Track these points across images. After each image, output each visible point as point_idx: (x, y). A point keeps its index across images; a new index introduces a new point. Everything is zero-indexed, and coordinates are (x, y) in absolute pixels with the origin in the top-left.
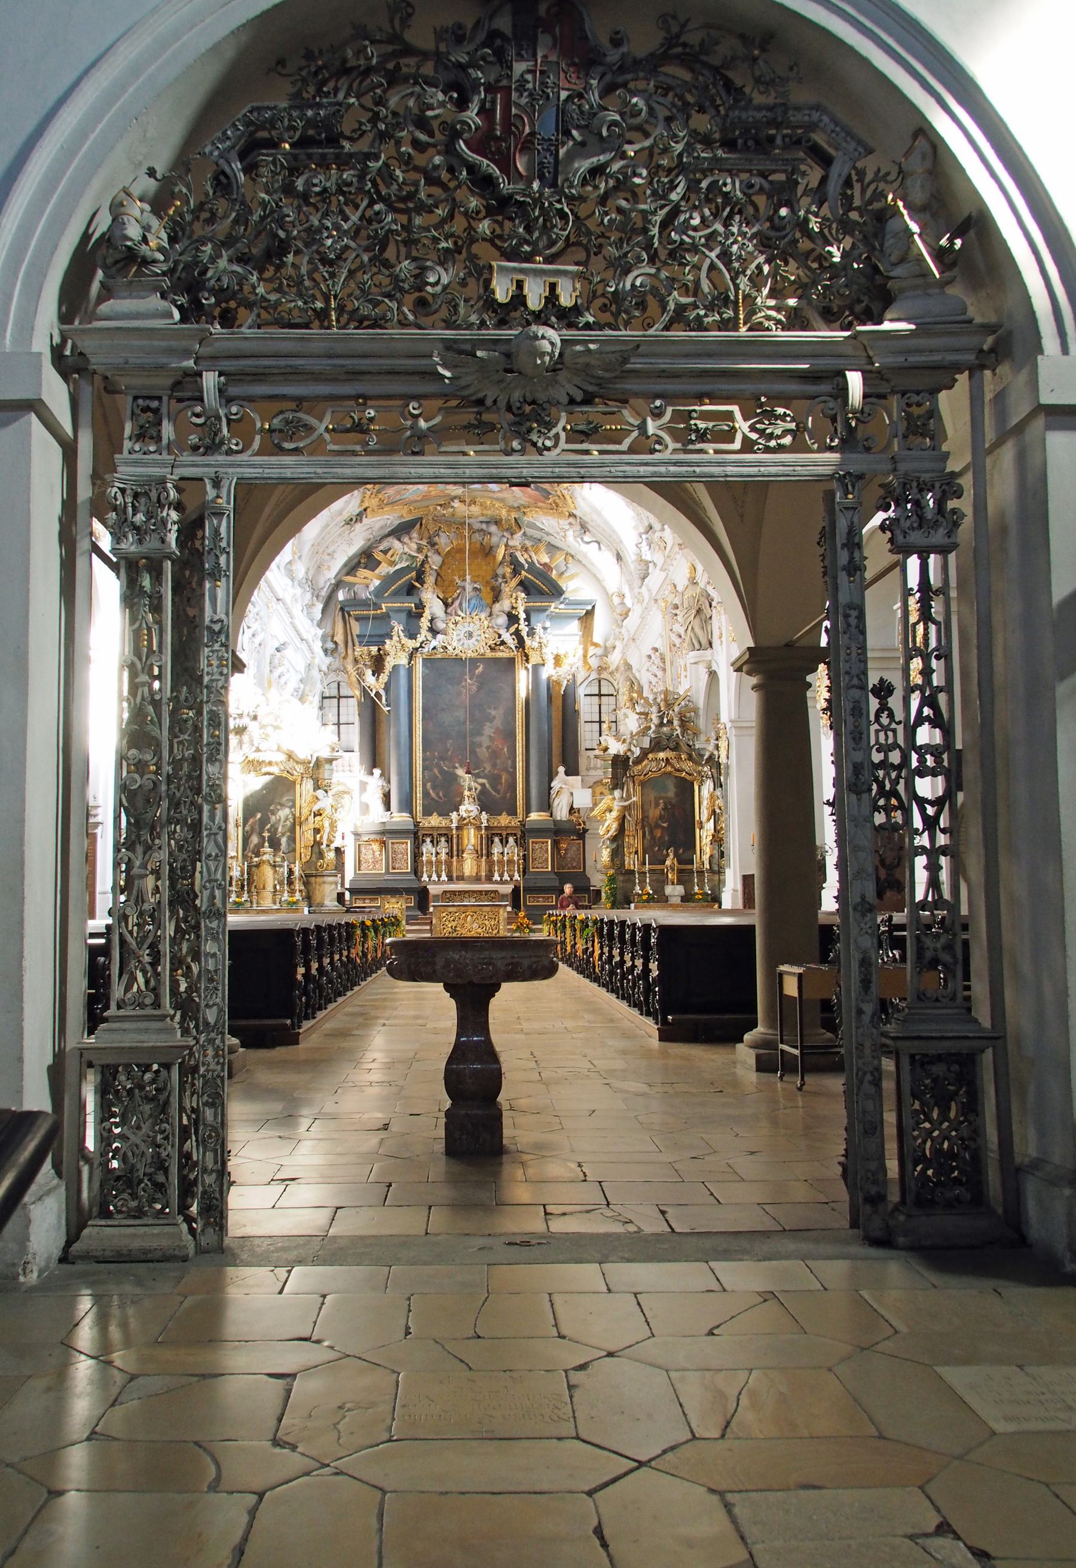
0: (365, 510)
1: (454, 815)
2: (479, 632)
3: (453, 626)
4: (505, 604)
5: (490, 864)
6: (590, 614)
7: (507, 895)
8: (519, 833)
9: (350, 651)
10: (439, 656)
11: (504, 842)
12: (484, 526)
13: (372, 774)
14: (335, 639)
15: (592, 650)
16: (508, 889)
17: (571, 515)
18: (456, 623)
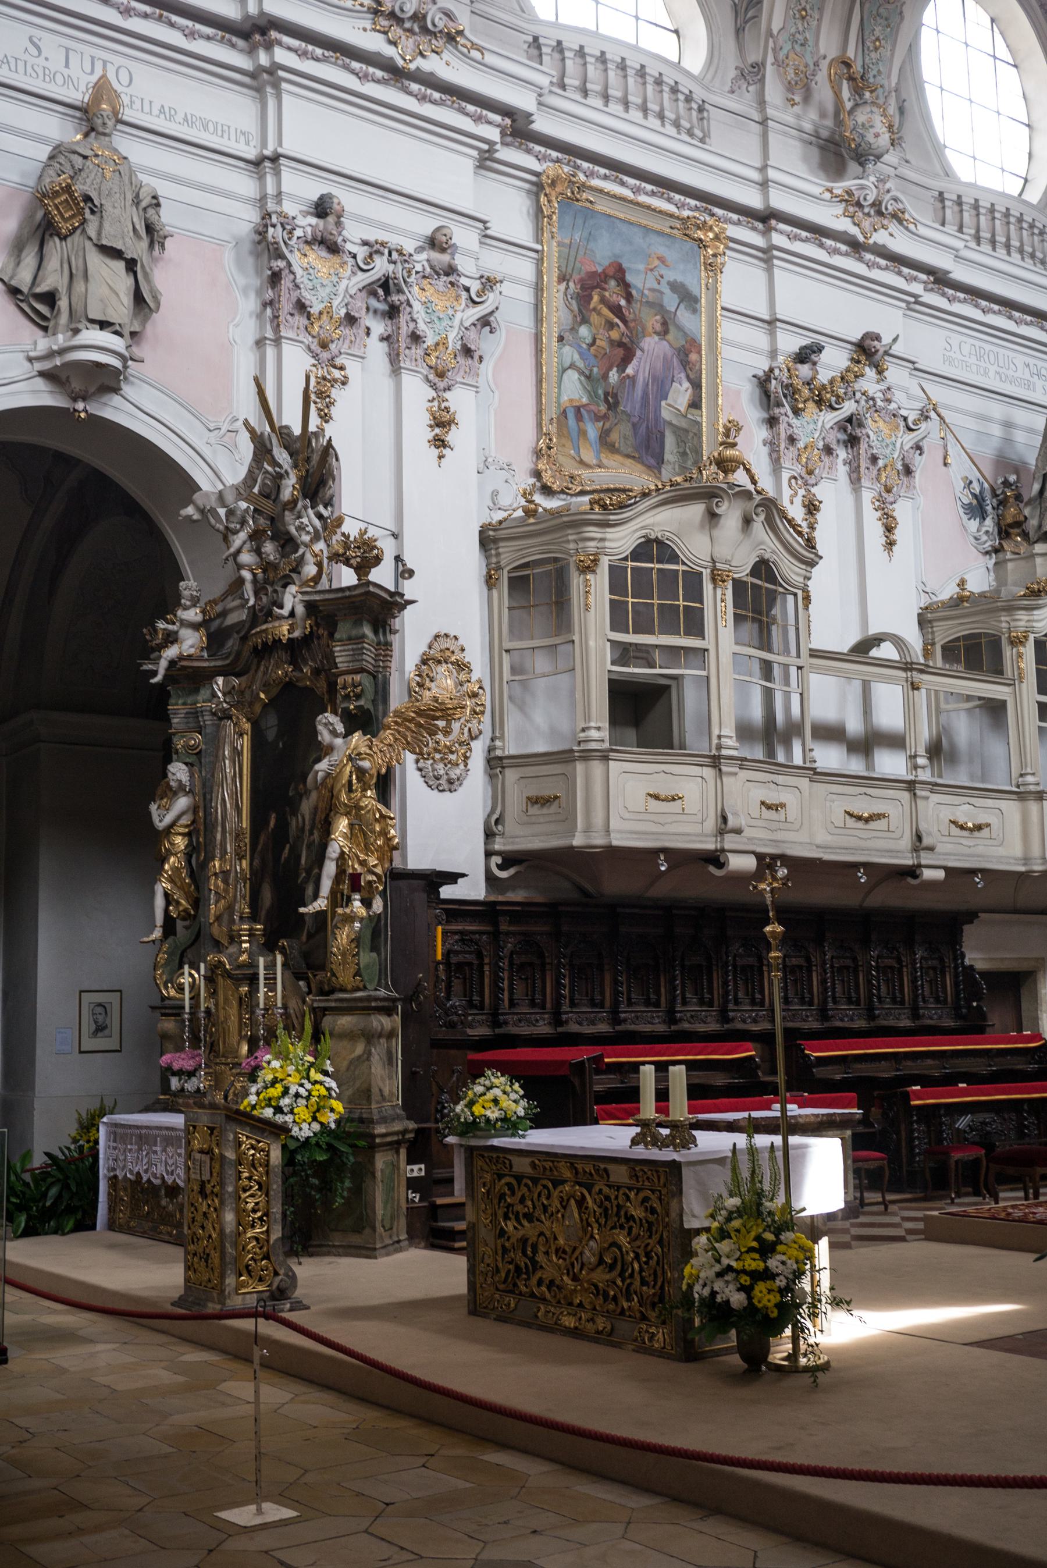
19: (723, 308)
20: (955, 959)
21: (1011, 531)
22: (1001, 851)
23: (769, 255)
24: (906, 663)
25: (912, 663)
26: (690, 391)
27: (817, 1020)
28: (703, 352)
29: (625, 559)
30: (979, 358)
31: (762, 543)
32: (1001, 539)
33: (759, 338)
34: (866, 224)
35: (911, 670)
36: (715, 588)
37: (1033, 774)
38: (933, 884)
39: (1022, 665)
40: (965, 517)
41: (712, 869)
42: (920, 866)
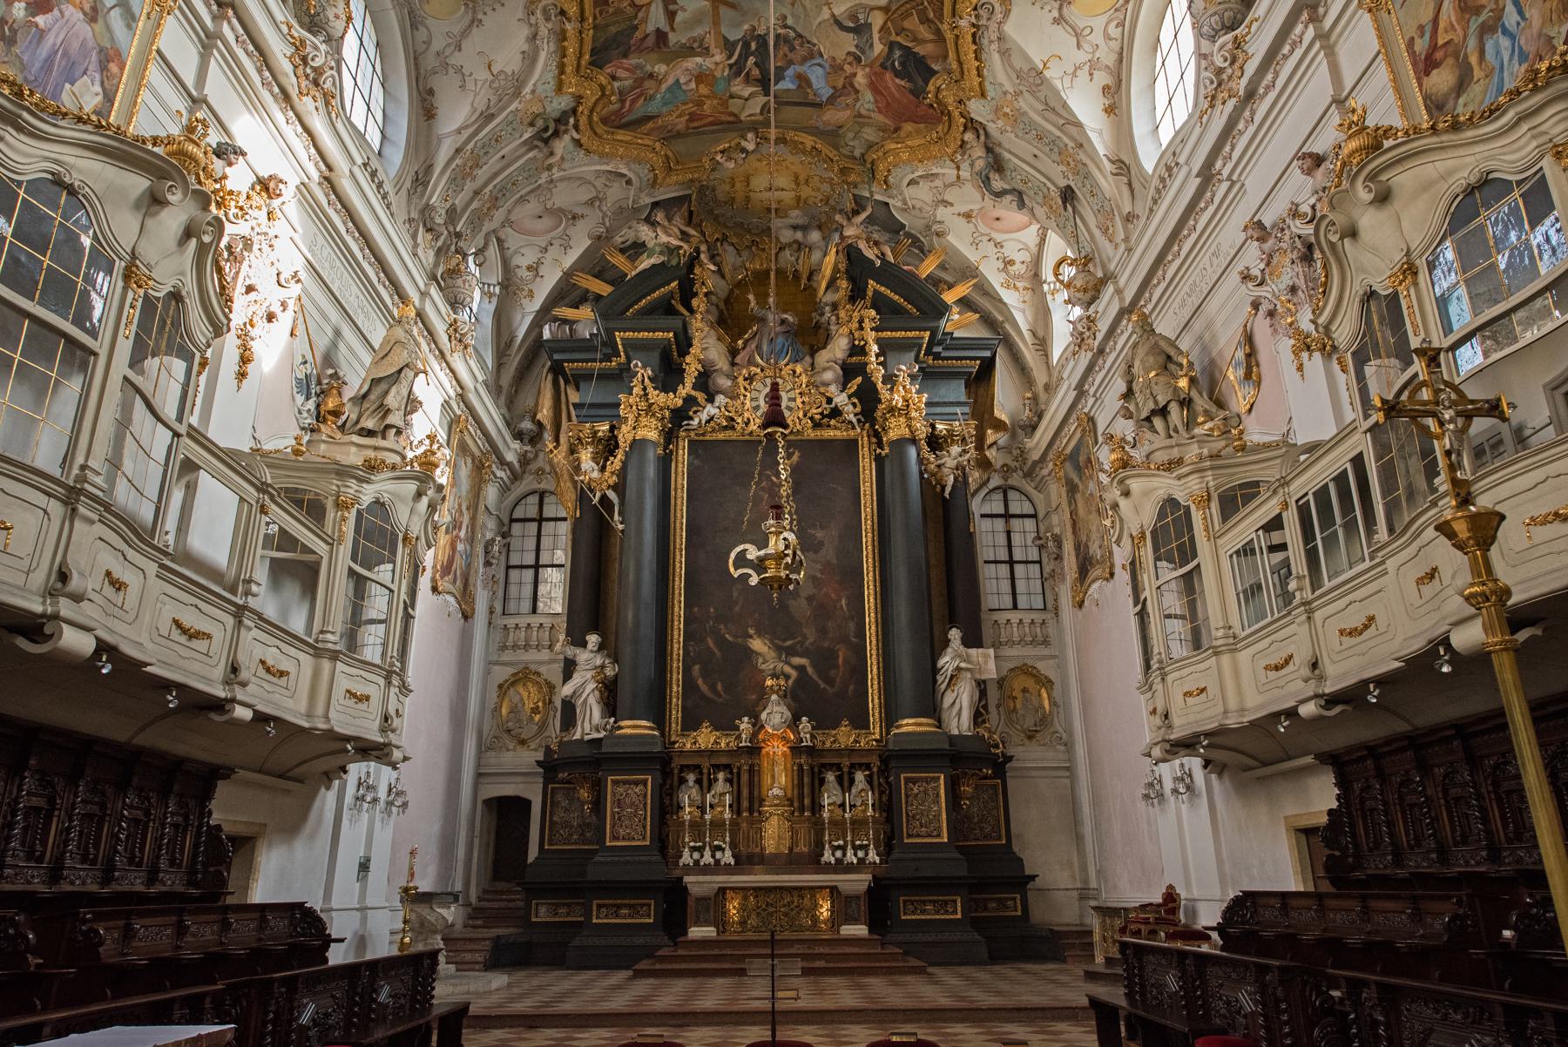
0: (574, 111)
1: (745, 725)
2: (791, 394)
3: (746, 384)
4: (839, 347)
5: (818, 826)
6: (988, 366)
7: (858, 897)
8: (876, 763)
9: (563, 439)
10: (721, 436)
11: (846, 783)
12: (799, 235)
13: (584, 644)
14: (539, 416)
15: (991, 435)
16: (857, 883)
17: (971, 125)
18: (750, 379)
19: (159, 52)
20: (202, 815)
21: (330, 417)
22: (290, 703)
23: (211, 41)
24: (263, 483)
25: (269, 485)
26: (100, 98)
27: (43, 882)
28: (126, 71)
29: (19, 184)
30: (332, 268)
31: (183, 273)
32: (318, 421)
33: (179, 103)
34: (304, 83)
35: (265, 492)
36: (125, 288)
37: (333, 633)
38: (239, 723)
39: (344, 529)
40: (295, 390)
41: (22, 643)
42: (233, 700)
